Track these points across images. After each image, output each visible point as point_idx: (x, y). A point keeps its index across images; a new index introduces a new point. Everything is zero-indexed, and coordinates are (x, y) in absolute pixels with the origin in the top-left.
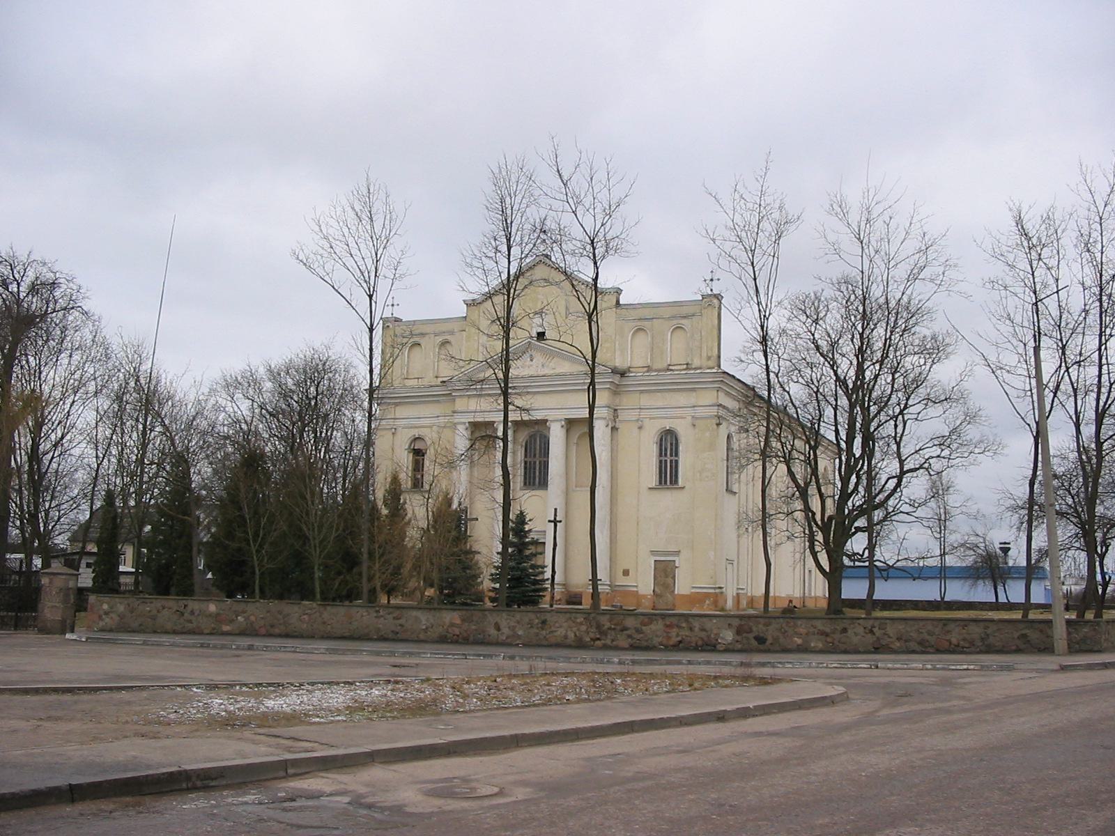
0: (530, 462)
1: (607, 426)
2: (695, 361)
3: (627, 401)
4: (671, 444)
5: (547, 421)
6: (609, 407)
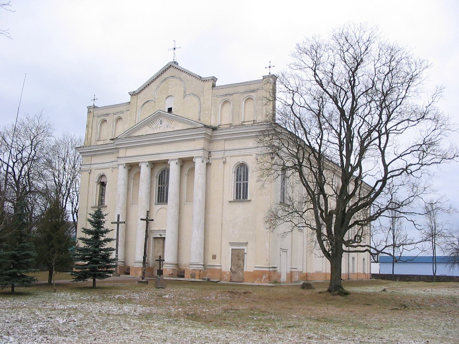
0: (161, 187)
1: (202, 162)
2: (259, 119)
3: (218, 146)
4: (244, 173)
5: (168, 160)
6: (203, 149)
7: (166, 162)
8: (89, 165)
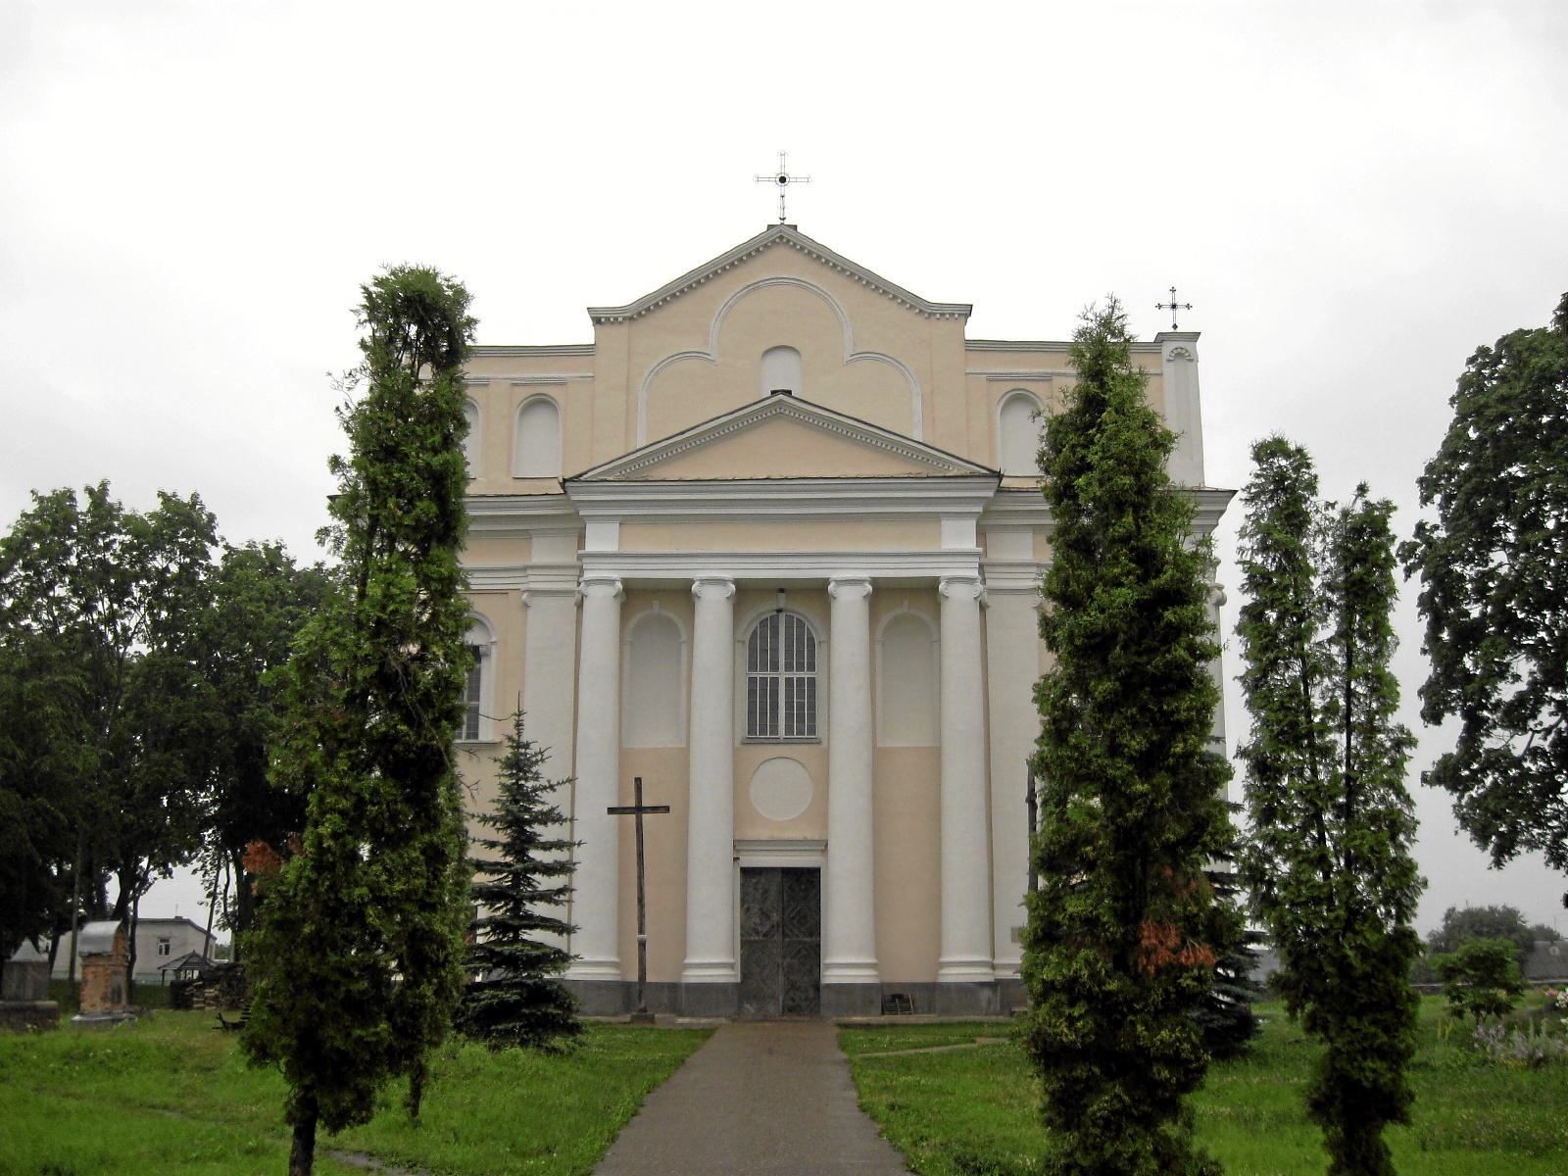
5: (826, 582)
7: (818, 592)
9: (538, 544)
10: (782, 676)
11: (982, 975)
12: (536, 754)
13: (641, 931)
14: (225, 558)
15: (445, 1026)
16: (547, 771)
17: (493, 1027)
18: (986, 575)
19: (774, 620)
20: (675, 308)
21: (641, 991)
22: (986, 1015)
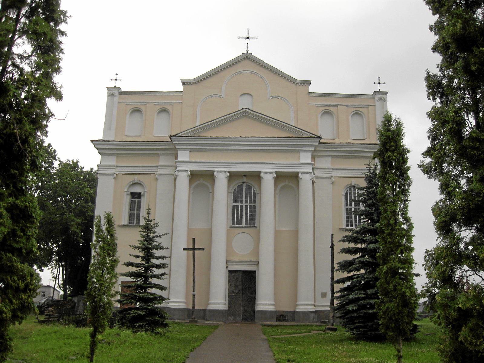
7: (257, 176)
8: (115, 168)
9: (161, 158)
10: (244, 205)
11: (313, 309)
12: (154, 224)
13: (194, 291)
14: (59, 165)
15: (106, 325)
16: (158, 231)
17: (135, 324)
18: (315, 172)
19: (242, 186)
20: (211, 80)
21: (193, 312)
22: (313, 322)
